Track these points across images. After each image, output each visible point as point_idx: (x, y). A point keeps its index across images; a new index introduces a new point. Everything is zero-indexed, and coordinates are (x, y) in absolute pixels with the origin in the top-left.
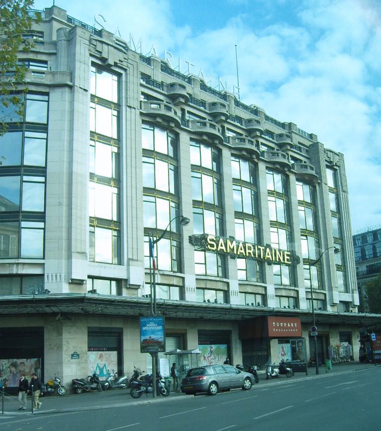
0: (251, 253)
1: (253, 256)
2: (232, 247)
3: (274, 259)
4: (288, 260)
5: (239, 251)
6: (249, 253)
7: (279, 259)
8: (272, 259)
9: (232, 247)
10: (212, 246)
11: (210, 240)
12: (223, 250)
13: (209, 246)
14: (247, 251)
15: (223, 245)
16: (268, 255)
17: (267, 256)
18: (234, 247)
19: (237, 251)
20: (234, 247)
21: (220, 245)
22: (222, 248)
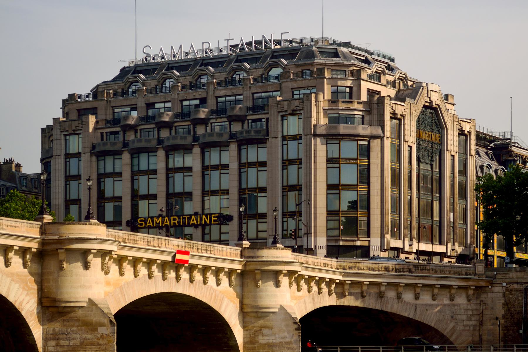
0: (176, 223)
1: (177, 225)
2: (158, 222)
3: (199, 223)
4: (214, 221)
5: (165, 223)
6: (175, 223)
7: (205, 221)
8: (197, 222)
9: (158, 222)
10: (142, 224)
11: (141, 221)
12: (151, 225)
13: (139, 225)
14: (172, 222)
15: (151, 221)
16: (193, 220)
17: (192, 222)
18: (160, 222)
19: (163, 223)
20: (160, 222)
21: (148, 222)
22: (149, 224)
